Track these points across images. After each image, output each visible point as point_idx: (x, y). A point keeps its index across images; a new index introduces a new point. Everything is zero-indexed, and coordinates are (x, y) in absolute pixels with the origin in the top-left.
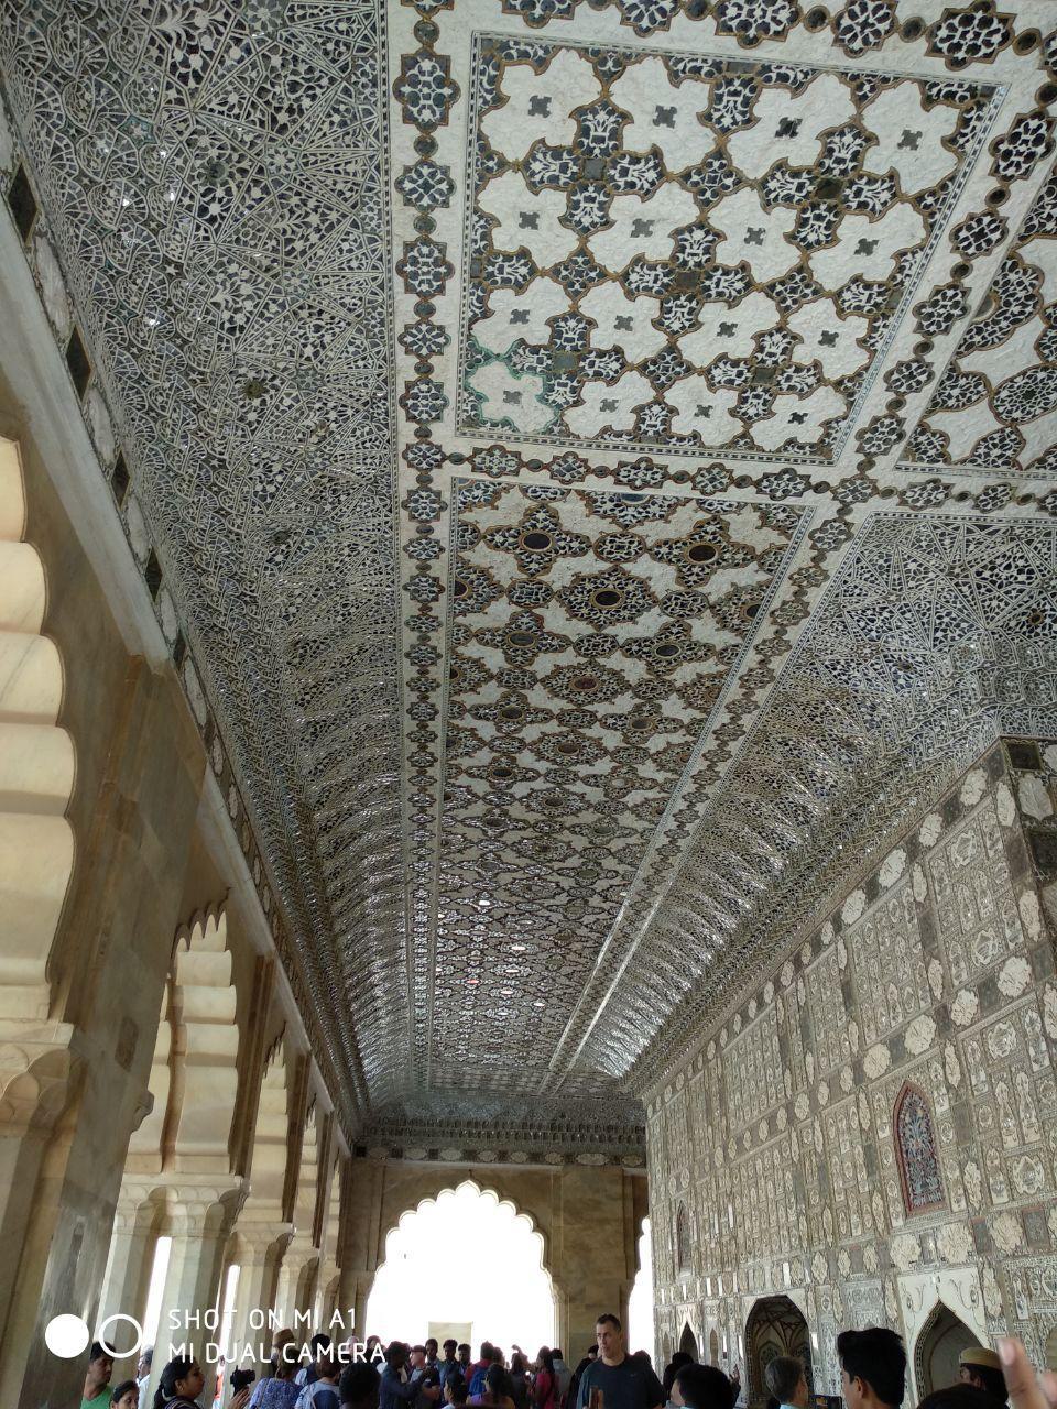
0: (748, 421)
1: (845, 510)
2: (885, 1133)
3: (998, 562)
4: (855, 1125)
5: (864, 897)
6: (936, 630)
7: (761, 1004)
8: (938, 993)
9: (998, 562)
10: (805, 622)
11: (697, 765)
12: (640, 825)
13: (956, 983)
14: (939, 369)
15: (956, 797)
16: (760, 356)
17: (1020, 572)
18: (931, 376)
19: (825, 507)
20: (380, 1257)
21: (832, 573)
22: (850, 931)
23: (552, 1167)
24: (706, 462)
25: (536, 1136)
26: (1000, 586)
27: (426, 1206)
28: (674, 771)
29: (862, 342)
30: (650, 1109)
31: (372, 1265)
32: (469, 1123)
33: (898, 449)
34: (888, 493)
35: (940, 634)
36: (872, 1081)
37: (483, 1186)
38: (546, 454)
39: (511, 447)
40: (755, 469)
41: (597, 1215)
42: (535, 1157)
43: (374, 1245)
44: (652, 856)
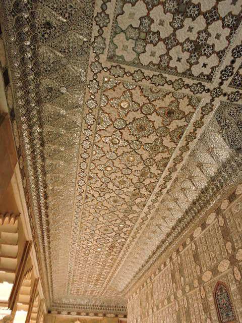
0: (191, 65)
1: (213, 100)
2: (211, 299)
4: (199, 297)
5: (200, 228)
7: (165, 265)
8: (230, 252)
11: (157, 189)
12: (138, 210)
13: (237, 248)
15: (234, 193)
16: (198, 40)
22: (196, 239)
24: (177, 78)
28: (150, 192)
30: (129, 300)
33: (230, 79)
34: (225, 95)
35: (232, 143)
36: (205, 282)
38: (132, 69)
39: (122, 66)
42: (96, 315)
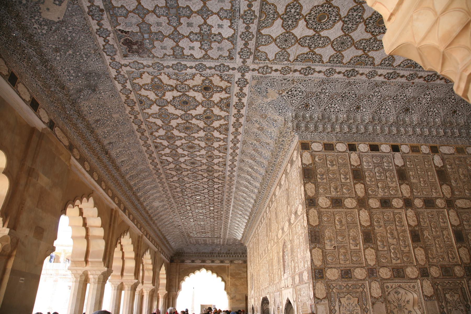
1: (243, 75)
3: (293, 89)
6: (279, 110)
9: (293, 89)
10: (244, 108)
14: (254, 33)
17: (300, 92)
18: (253, 36)
19: (238, 75)
20: (179, 288)
21: (247, 93)
23: (227, 264)
25: (222, 256)
26: (295, 96)
27: (192, 275)
28: (224, 153)
29: (230, 27)
31: (177, 290)
32: (203, 253)
35: (280, 111)
37: (207, 270)
40: (213, 64)
41: (239, 276)
42: (222, 262)
43: (177, 285)
44: (227, 178)
